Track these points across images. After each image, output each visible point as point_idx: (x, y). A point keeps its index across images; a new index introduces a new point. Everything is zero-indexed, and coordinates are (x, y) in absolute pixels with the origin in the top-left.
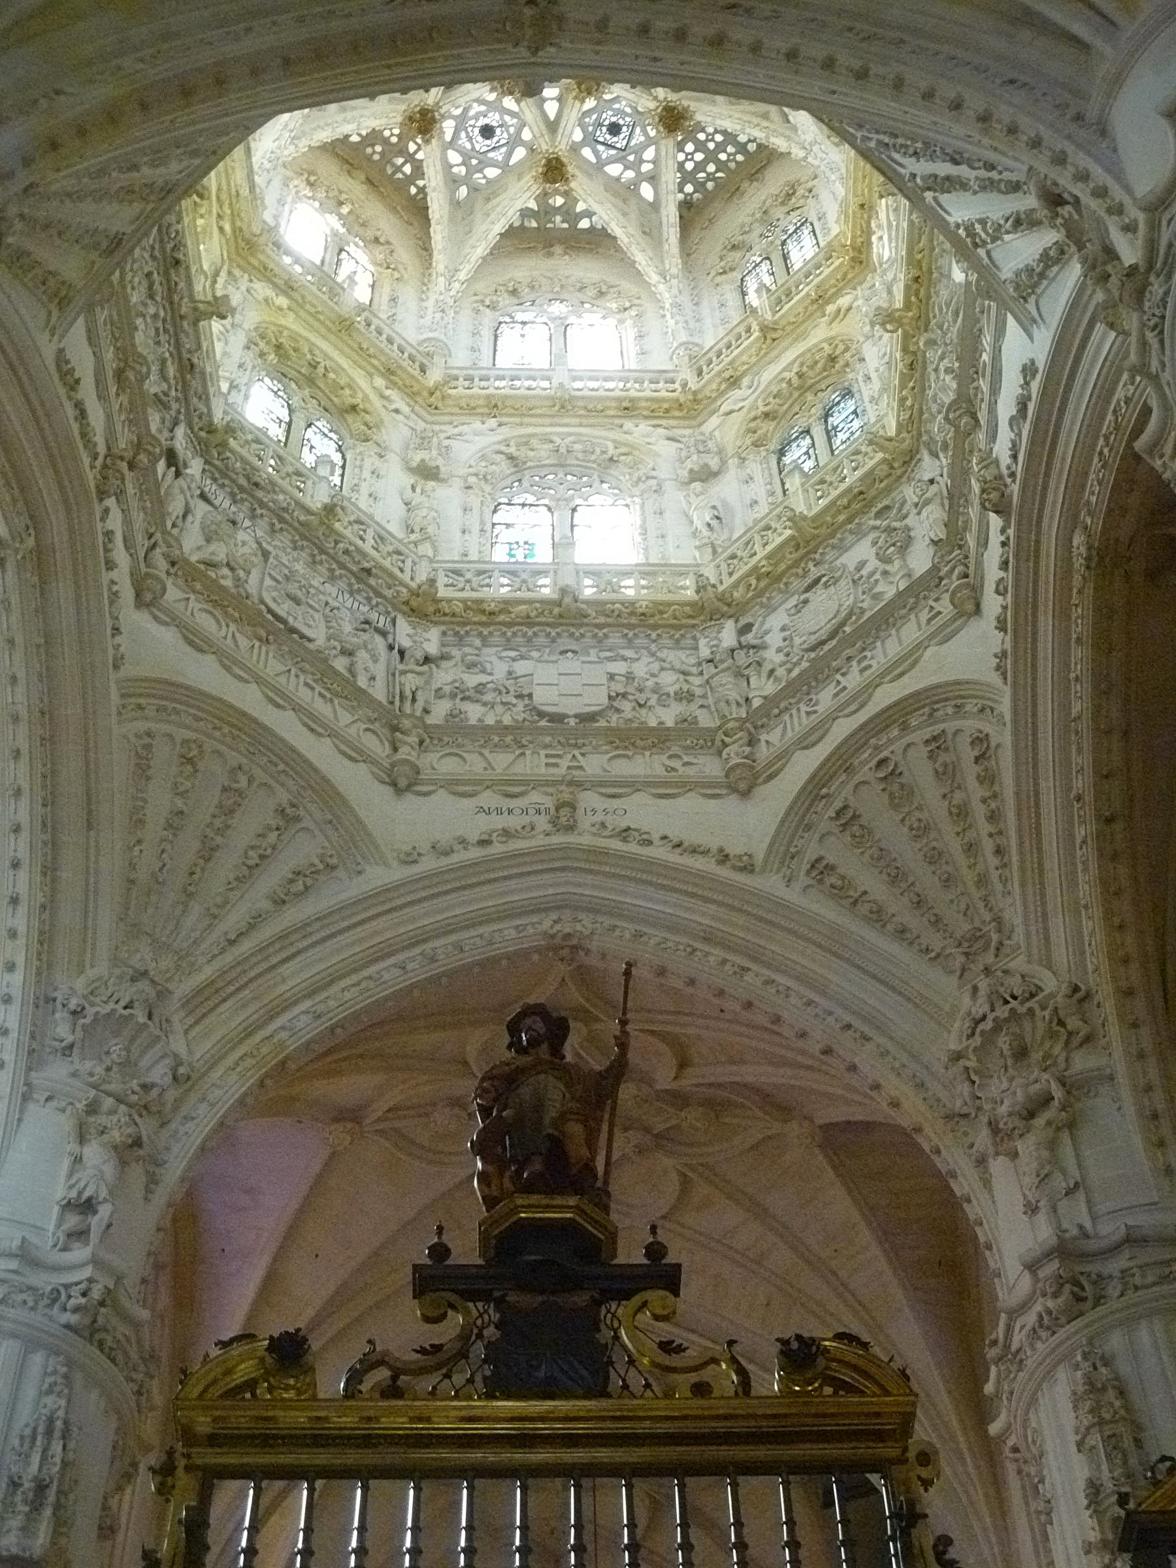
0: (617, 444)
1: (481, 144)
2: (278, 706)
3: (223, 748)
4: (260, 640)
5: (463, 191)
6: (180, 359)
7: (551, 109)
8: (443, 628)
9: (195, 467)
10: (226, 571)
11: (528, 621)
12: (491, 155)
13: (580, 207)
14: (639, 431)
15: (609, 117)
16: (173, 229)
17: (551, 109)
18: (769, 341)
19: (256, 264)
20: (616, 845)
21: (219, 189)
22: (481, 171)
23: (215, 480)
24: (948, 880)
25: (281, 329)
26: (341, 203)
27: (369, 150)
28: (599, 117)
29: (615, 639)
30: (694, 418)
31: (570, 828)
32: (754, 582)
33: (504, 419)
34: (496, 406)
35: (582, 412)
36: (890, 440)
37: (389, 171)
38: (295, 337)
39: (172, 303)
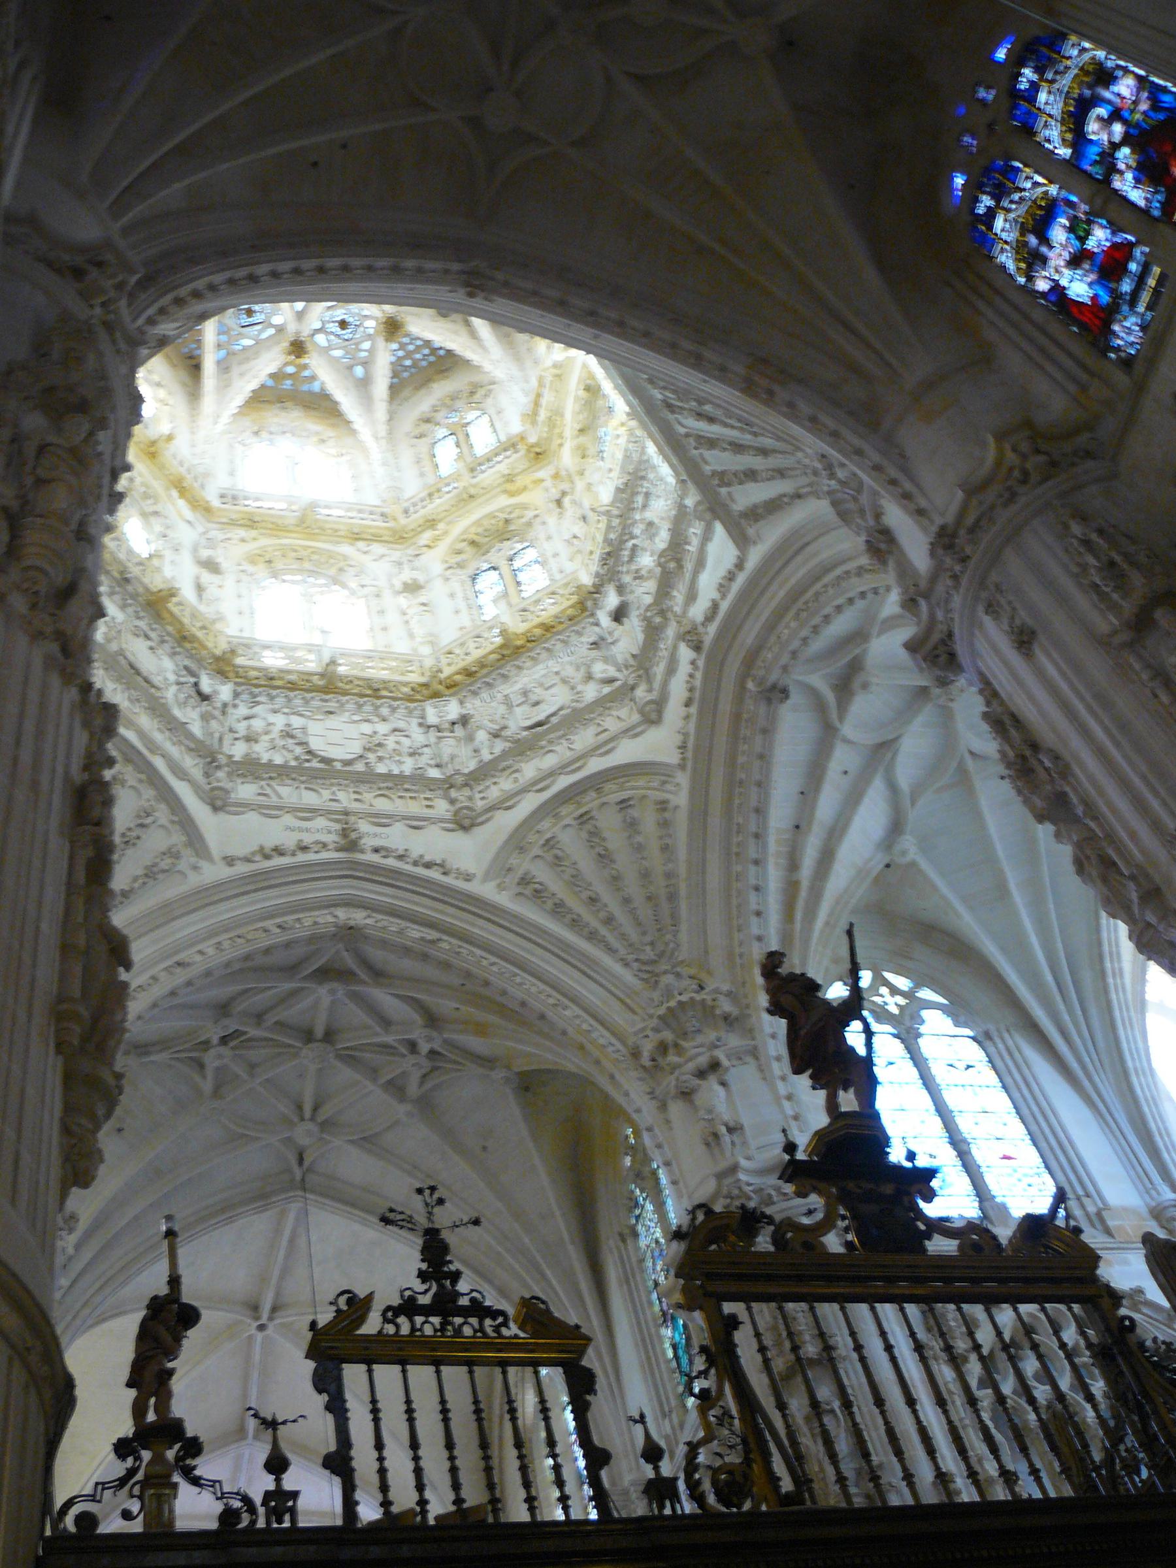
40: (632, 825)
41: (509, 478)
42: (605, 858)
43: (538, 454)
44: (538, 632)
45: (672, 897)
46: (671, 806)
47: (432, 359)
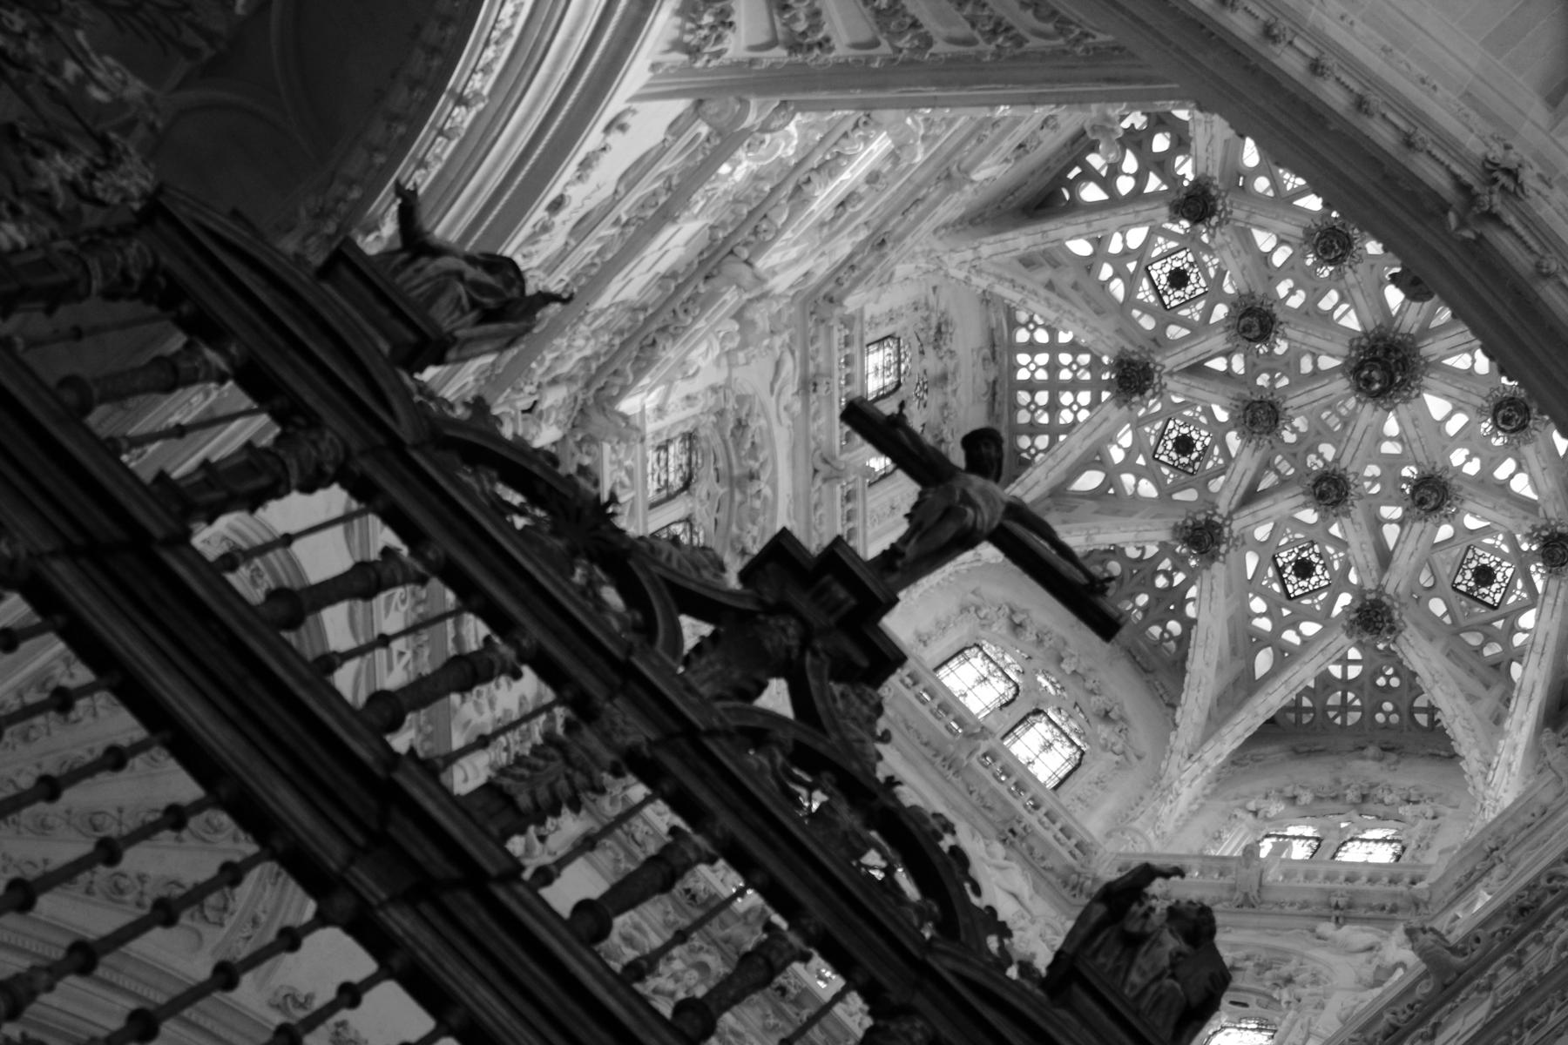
13: (1130, 163)
15: (1197, 284)
18: (820, 466)
28: (1206, 276)
30: (804, 303)
35: (923, 192)
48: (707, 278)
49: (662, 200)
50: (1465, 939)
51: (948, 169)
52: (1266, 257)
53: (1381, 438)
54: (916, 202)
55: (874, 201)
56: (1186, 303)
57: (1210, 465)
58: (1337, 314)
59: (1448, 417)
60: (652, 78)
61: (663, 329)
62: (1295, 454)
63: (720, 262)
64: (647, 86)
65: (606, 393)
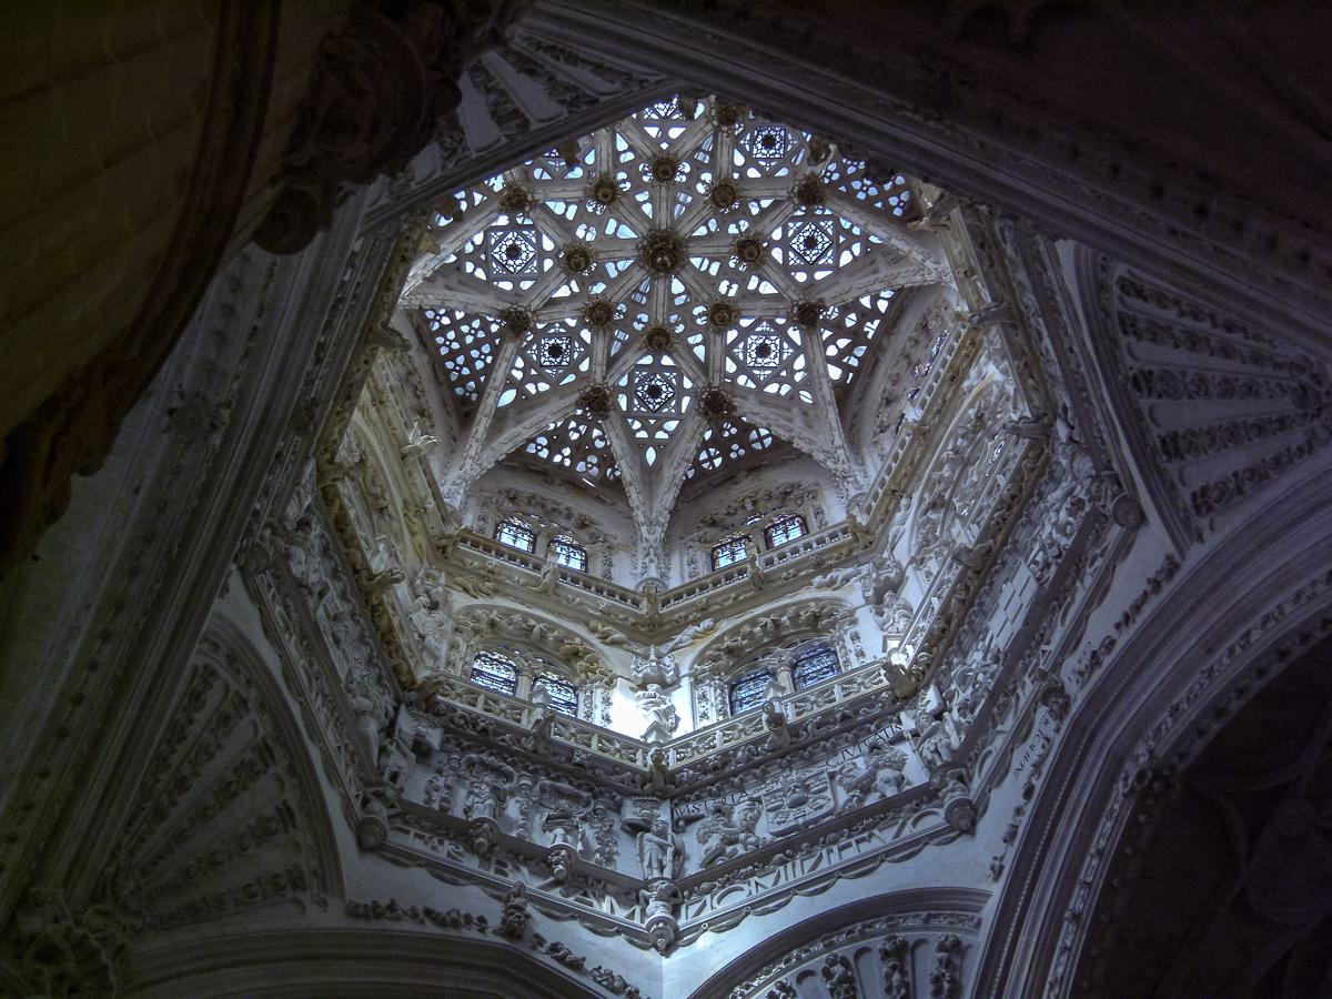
0: (971, 405)
1: (772, 360)
2: (825, 889)
3: (804, 967)
4: (783, 863)
5: (806, 397)
6: (570, 771)
7: (767, 289)
8: (934, 680)
9: (664, 814)
10: (729, 849)
11: (966, 604)
12: (785, 356)
13: (866, 302)
14: (971, 381)
15: (798, 243)
16: (456, 720)
17: (767, 289)
19: (668, 627)
20: (1098, 673)
21: (587, 624)
22: (794, 372)
23: (688, 801)
24: (1250, 389)
25: (720, 639)
26: (743, 507)
27: (733, 455)
29: (1022, 535)
31: (1065, 707)
32: (1030, 381)
33: (909, 492)
34: (894, 491)
35: (936, 420)
36: (942, 196)
37: (757, 446)
38: (734, 632)
39: (517, 753)
40: (262, 832)
41: (421, 511)
42: (226, 792)
43: (444, 549)
44: (384, 622)
45: (195, 913)
46: (301, 895)
47: (444, 351)
48: (990, 551)
49: (995, 710)
50: (374, 356)
51: (925, 439)
52: (761, 280)
53: (650, 200)
54: (939, 412)
55: (960, 420)
56: (800, 230)
57: (748, 137)
58: (706, 262)
59: (617, 229)
60: (978, 910)
61: (1010, 508)
62: (698, 168)
63: (984, 565)
64: (984, 902)
65: (1037, 452)
